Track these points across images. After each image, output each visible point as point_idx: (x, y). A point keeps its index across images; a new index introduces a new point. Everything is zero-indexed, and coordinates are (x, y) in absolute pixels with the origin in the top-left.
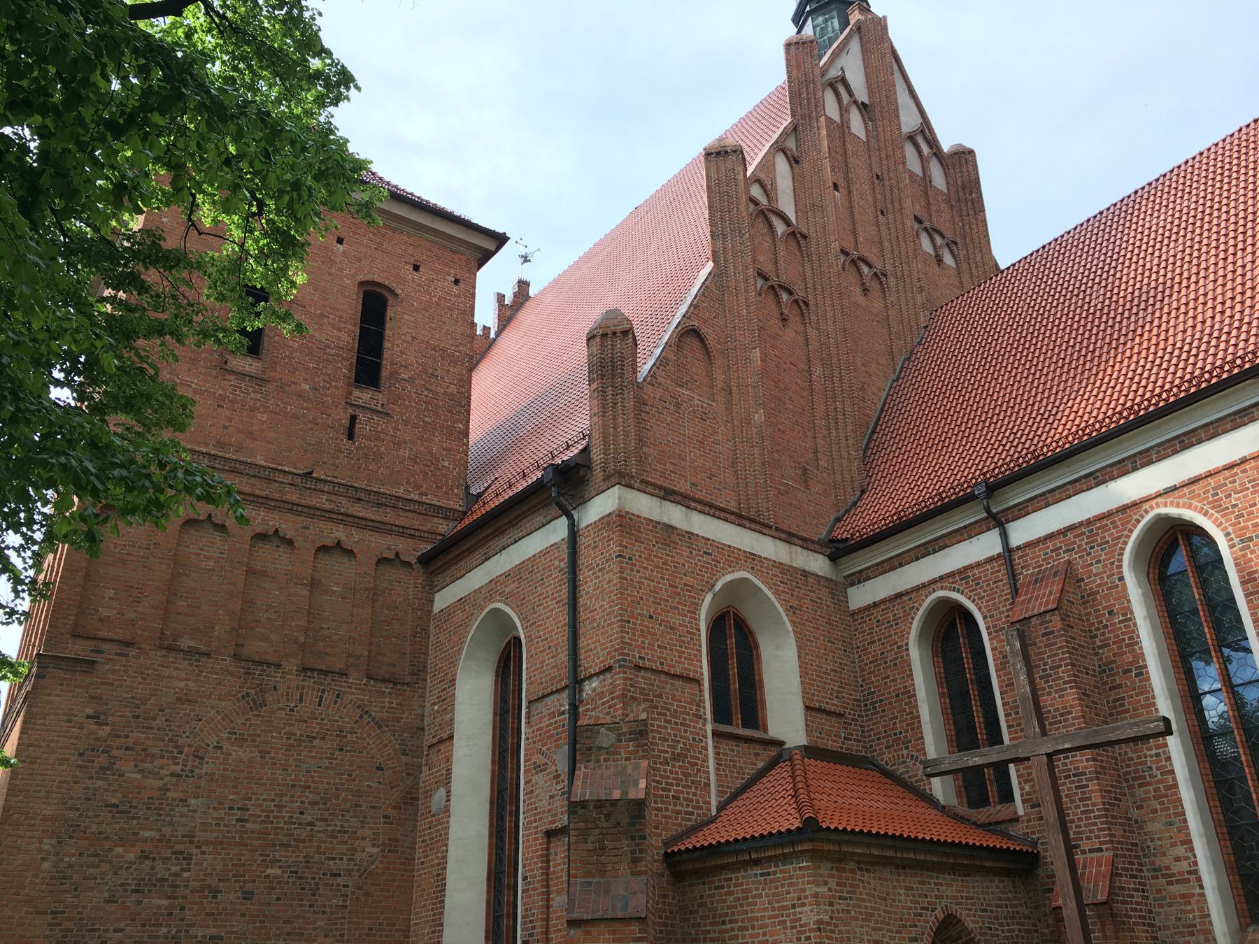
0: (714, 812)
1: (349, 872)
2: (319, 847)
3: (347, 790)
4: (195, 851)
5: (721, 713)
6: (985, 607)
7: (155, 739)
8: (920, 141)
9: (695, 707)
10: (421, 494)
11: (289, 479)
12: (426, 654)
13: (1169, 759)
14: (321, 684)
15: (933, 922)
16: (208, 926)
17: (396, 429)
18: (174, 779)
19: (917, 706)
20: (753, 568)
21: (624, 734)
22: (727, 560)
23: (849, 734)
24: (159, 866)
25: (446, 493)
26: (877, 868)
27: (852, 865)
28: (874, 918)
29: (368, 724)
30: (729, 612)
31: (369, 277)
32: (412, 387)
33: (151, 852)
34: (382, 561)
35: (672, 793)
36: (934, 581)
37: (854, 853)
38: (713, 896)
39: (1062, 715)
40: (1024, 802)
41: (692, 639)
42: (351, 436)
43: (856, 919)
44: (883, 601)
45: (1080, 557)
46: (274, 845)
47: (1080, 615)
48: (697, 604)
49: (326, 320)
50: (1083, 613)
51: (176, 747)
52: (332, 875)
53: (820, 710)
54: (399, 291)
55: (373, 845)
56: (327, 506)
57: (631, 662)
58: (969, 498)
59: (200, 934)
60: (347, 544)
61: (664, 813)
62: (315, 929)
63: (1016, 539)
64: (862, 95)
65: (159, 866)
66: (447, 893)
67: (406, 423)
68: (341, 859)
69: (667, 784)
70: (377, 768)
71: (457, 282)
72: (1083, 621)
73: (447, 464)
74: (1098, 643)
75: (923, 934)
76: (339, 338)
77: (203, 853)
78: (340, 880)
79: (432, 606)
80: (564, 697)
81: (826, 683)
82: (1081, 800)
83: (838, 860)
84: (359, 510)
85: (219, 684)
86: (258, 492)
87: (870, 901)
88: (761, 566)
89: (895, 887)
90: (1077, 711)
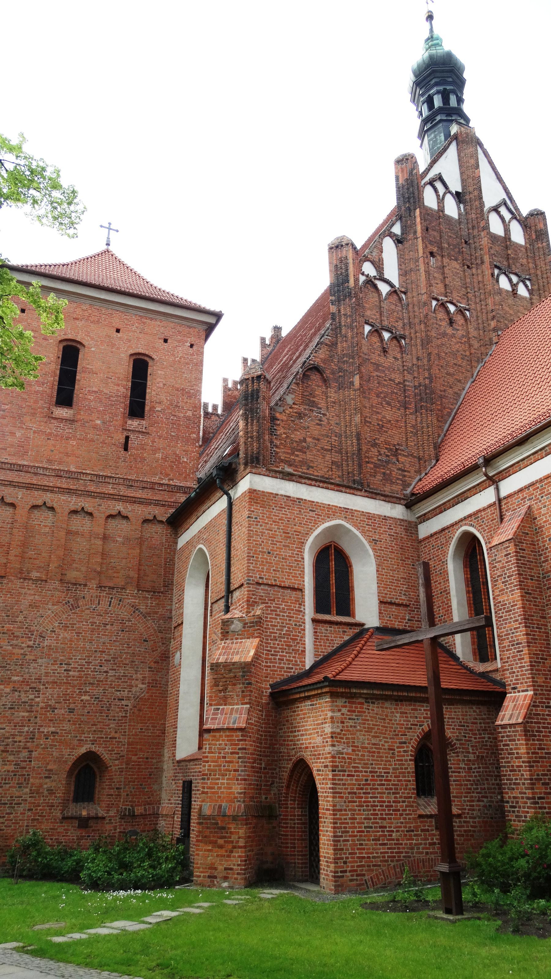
0: (307, 667)
1: (128, 698)
2: (111, 684)
3: (127, 653)
4: (42, 687)
6: (487, 536)
7: (18, 628)
8: (503, 211)
9: (297, 606)
10: (169, 480)
11: (89, 478)
12: (173, 574)
14: (110, 594)
15: (420, 733)
16: (50, 727)
17: (153, 442)
18: (30, 649)
19: (450, 600)
20: (346, 518)
21: (247, 623)
22: (326, 514)
23: (412, 617)
24: (23, 695)
25: (185, 478)
26: (380, 701)
28: (374, 731)
29: (138, 615)
30: (331, 545)
31: (137, 351)
32: (164, 415)
33: (18, 688)
34: (146, 521)
36: (461, 520)
37: (360, 694)
38: (291, 716)
39: (512, 606)
41: (298, 564)
42: (126, 449)
43: (361, 731)
44: (436, 533)
45: (536, 503)
46: (85, 684)
47: (533, 541)
48: (303, 543)
49: (110, 380)
50: (536, 539)
51: (30, 632)
52: (119, 700)
53: (391, 603)
54: (154, 357)
55: (143, 684)
56: (111, 492)
57: (253, 580)
58: (475, 468)
59: (46, 731)
60: (124, 512)
61: (272, 668)
62: (110, 729)
63: (504, 493)
64: (456, 186)
65: (23, 695)
66: (179, 710)
67: (160, 437)
68: (124, 691)
69: (275, 651)
70: (144, 641)
71: (192, 346)
72: (535, 545)
73: (185, 460)
74: (543, 559)
75: (411, 739)
76: (118, 390)
77: (46, 688)
78: (123, 702)
79: (176, 546)
80: (223, 600)
81: (396, 586)
82: (519, 659)
83: (351, 697)
84: (131, 493)
85: (53, 596)
86: (71, 487)
87: (372, 721)
88: (352, 516)
90: (519, 604)
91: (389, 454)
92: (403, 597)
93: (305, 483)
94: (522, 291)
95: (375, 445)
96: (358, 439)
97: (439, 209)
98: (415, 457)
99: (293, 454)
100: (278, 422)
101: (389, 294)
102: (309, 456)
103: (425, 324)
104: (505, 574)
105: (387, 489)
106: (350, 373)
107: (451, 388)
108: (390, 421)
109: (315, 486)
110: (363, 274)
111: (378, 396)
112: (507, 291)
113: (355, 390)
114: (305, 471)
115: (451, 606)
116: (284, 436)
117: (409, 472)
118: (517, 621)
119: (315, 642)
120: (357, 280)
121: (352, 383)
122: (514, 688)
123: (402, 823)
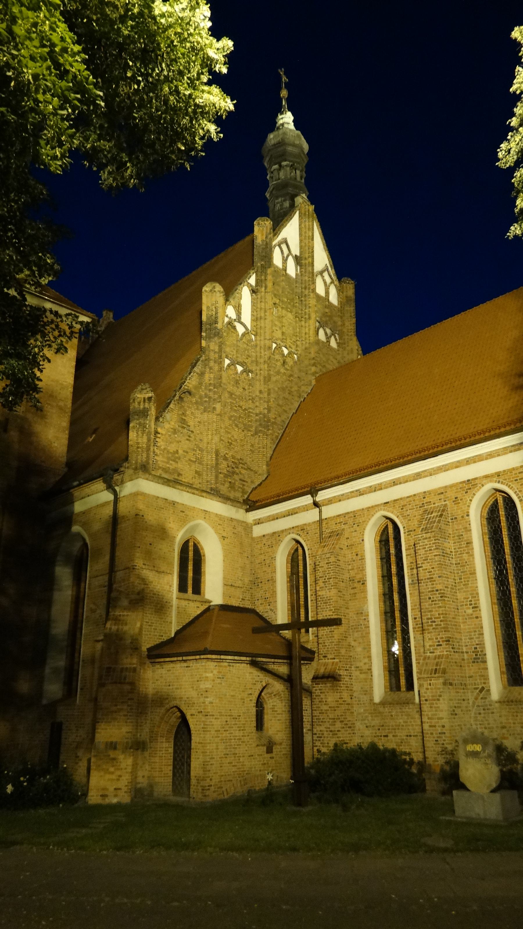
0: (173, 635)
5: (182, 588)
6: (310, 545)
8: (326, 274)
13: (368, 621)
20: (205, 518)
27: (226, 664)
35: (153, 627)
39: (329, 600)
40: (312, 634)
64: (296, 251)
69: (151, 623)
89: (244, 673)
91: (234, 466)
92: (240, 582)
93: (178, 489)
94: (333, 344)
95: (226, 459)
96: (217, 454)
97: (283, 269)
98: (252, 470)
99: (168, 463)
100: (159, 435)
101: (244, 335)
102: (180, 465)
103: (268, 364)
104: (326, 576)
105: (232, 495)
106: (214, 400)
107: (280, 416)
108: (236, 440)
109: (185, 491)
110: (227, 316)
111: (230, 419)
112: (323, 342)
113: (217, 415)
114: (176, 477)
115: (275, 592)
116: (162, 447)
117: (247, 482)
118: (332, 610)
119: (178, 615)
120: (224, 321)
121: (214, 408)
122: (325, 657)
123: (246, 751)
